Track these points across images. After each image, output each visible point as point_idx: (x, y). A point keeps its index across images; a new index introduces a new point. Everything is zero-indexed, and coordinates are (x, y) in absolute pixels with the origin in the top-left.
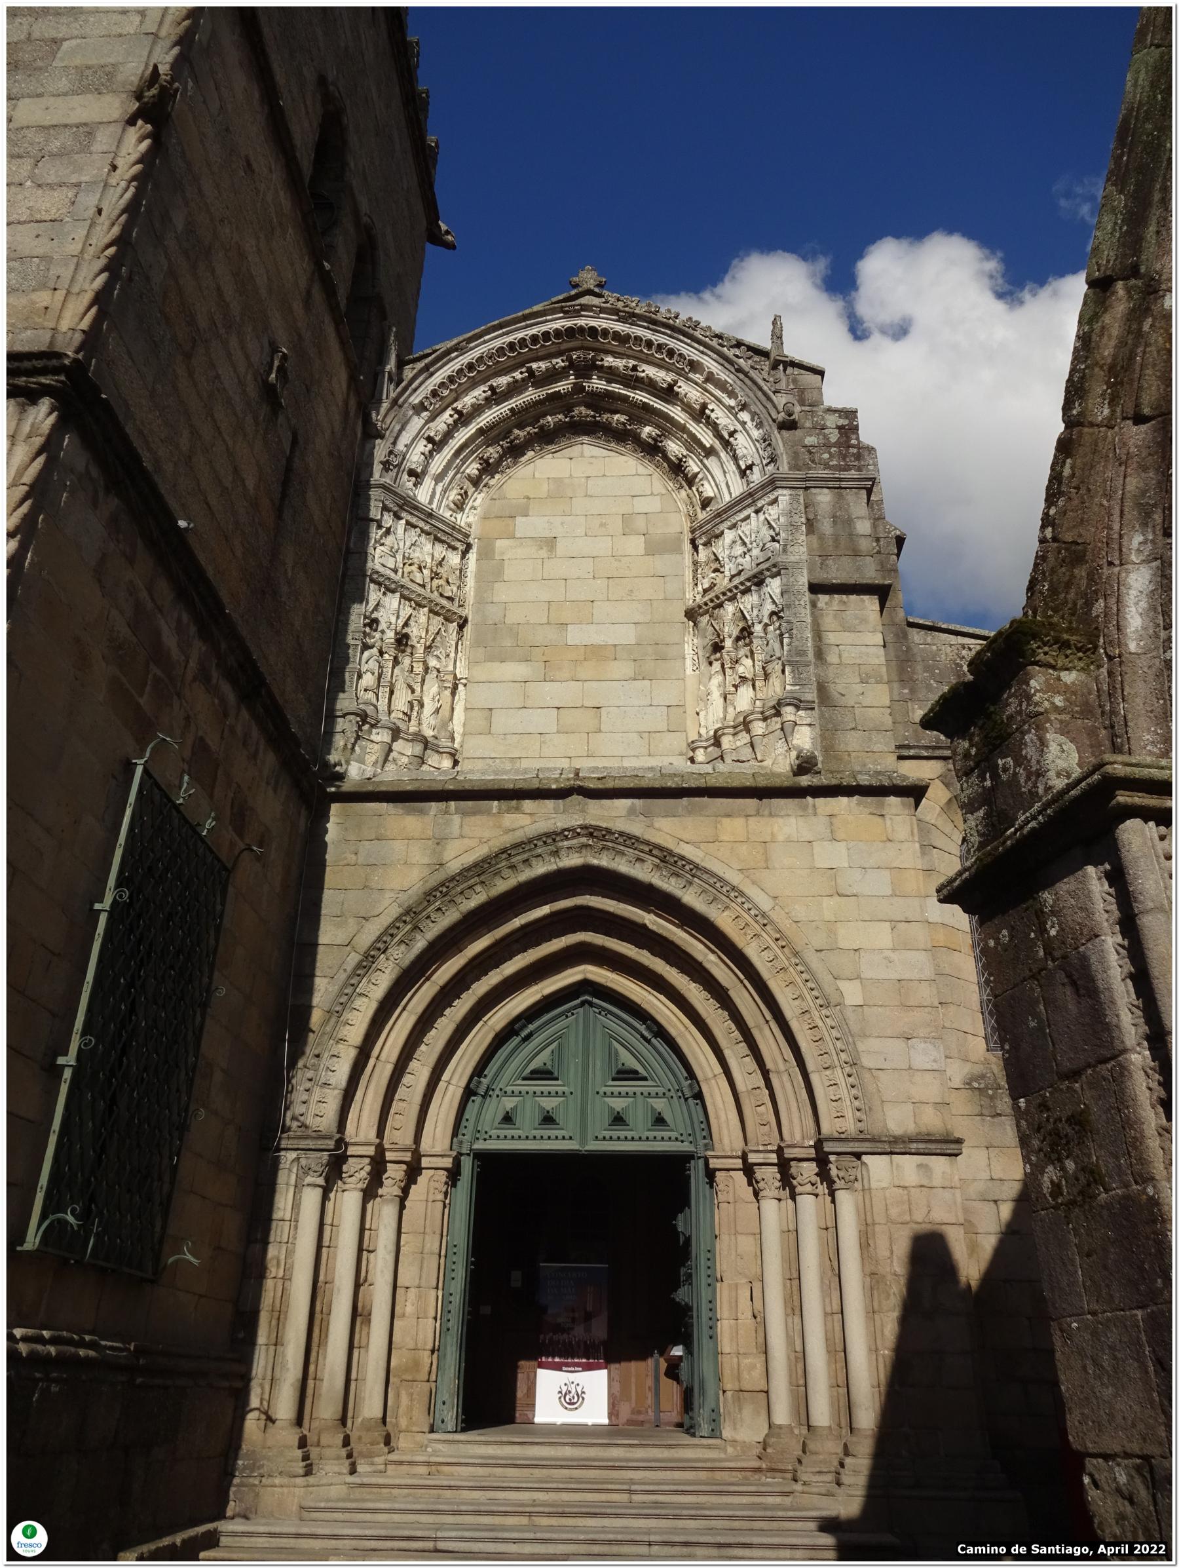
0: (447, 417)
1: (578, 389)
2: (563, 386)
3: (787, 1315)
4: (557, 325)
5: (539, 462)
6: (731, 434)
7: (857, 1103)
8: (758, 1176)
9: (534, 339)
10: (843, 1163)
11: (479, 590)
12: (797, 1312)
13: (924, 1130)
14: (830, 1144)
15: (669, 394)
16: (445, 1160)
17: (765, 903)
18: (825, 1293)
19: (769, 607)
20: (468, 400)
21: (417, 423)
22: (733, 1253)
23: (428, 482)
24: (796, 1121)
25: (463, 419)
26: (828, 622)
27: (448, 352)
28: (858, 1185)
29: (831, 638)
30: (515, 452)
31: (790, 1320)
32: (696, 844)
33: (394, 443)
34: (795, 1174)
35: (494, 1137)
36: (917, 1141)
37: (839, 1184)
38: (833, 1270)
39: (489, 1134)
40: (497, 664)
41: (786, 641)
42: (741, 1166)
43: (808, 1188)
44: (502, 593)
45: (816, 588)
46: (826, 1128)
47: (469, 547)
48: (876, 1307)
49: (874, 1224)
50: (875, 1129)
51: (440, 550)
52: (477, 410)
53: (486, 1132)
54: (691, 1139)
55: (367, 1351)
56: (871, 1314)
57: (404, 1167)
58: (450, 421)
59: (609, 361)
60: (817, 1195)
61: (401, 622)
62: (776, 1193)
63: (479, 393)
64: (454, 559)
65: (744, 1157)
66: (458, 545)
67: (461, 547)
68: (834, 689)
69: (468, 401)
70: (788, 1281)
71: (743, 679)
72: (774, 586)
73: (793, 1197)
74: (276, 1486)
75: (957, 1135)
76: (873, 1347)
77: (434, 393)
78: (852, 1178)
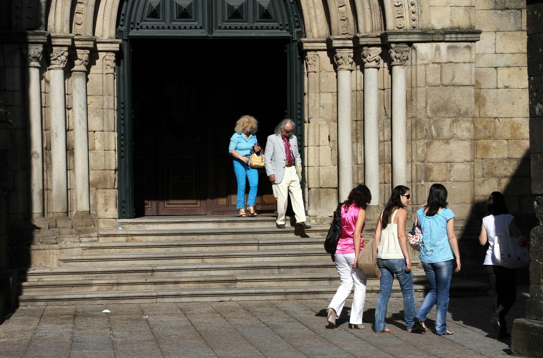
3: (353, 143)
7: (412, 8)
8: (339, 55)
10: (400, 49)
12: (361, 140)
13: (456, 25)
14: (392, 36)
16: (114, 45)
18: (381, 129)
22: (317, 105)
24: (368, 19)
28: (409, 62)
31: (355, 146)
34: (365, 55)
35: (144, 27)
36: (450, 33)
37: (396, 62)
38: (386, 115)
39: (140, 24)
42: (326, 48)
43: (374, 64)
46: (391, 25)
48: (414, 137)
49: (417, 87)
50: (423, 23)
53: (138, 24)
54: (288, 28)
55: (74, 172)
56: (410, 141)
57: (88, 52)
60: (378, 68)
62: (349, 67)
65: (329, 42)
70: (355, 122)
73: (362, 70)
74: (41, 250)
75: (477, 28)
76: (410, 160)
78: (405, 58)
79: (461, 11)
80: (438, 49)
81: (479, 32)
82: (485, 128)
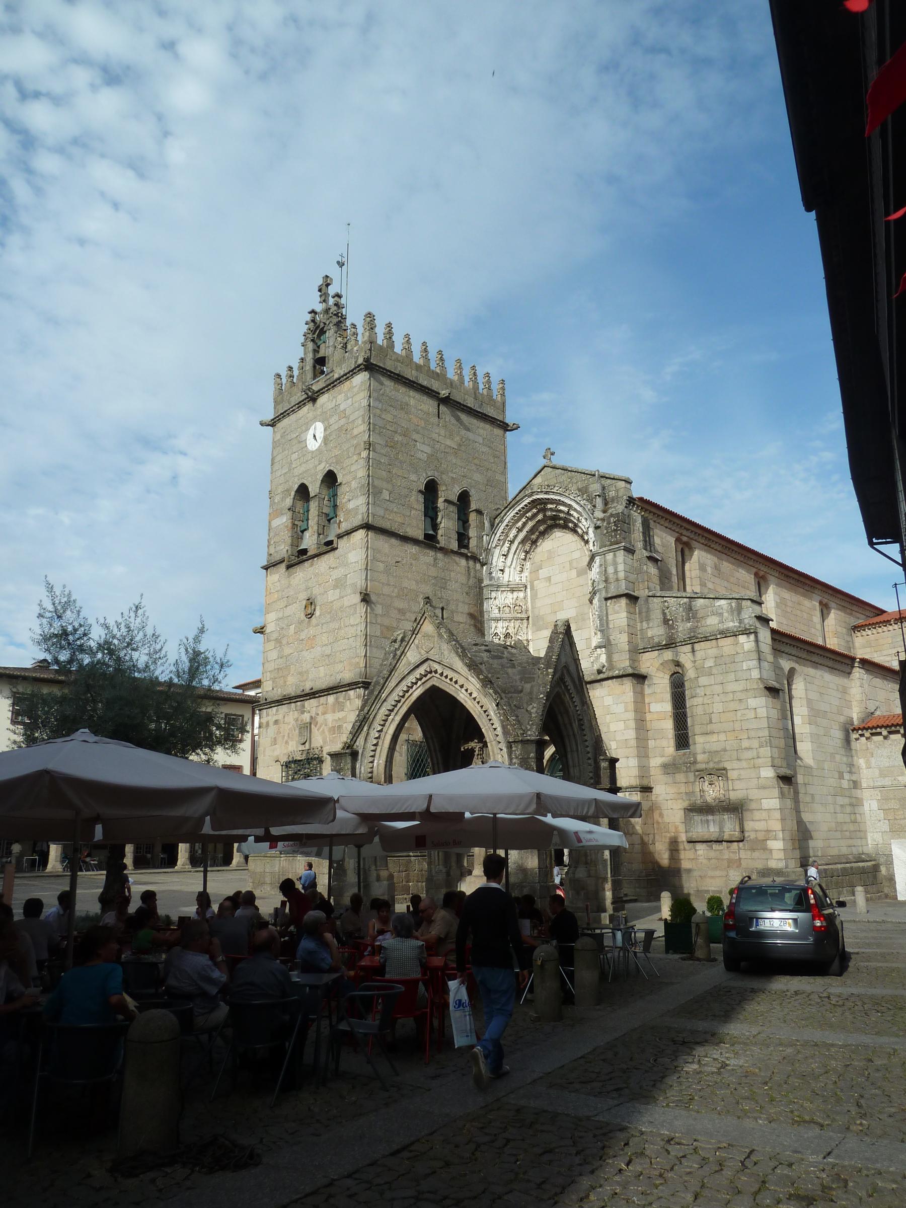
0: (507, 545)
1: (545, 516)
2: (540, 517)
4: (527, 501)
5: (544, 544)
9: (523, 508)
11: (532, 603)
13: (631, 784)
20: (511, 536)
21: (497, 552)
23: (507, 570)
25: (512, 542)
26: (610, 611)
27: (498, 524)
29: (610, 618)
30: (534, 542)
33: (491, 564)
40: (539, 632)
44: (538, 604)
45: (606, 599)
47: (526, 587)
51: (515, 594)
52: (516, 537)
58: (508, 545)
59: (550, 506)
61: (505, 629)
63: (514, 532)
64: (521, 595)
66: (522, 589)
67: (523, 589)
68: (611, 638)
69: (511, 536)
77: (499, 540)
79: (632, 778)
80: (625, 795)
82: (665, 827)
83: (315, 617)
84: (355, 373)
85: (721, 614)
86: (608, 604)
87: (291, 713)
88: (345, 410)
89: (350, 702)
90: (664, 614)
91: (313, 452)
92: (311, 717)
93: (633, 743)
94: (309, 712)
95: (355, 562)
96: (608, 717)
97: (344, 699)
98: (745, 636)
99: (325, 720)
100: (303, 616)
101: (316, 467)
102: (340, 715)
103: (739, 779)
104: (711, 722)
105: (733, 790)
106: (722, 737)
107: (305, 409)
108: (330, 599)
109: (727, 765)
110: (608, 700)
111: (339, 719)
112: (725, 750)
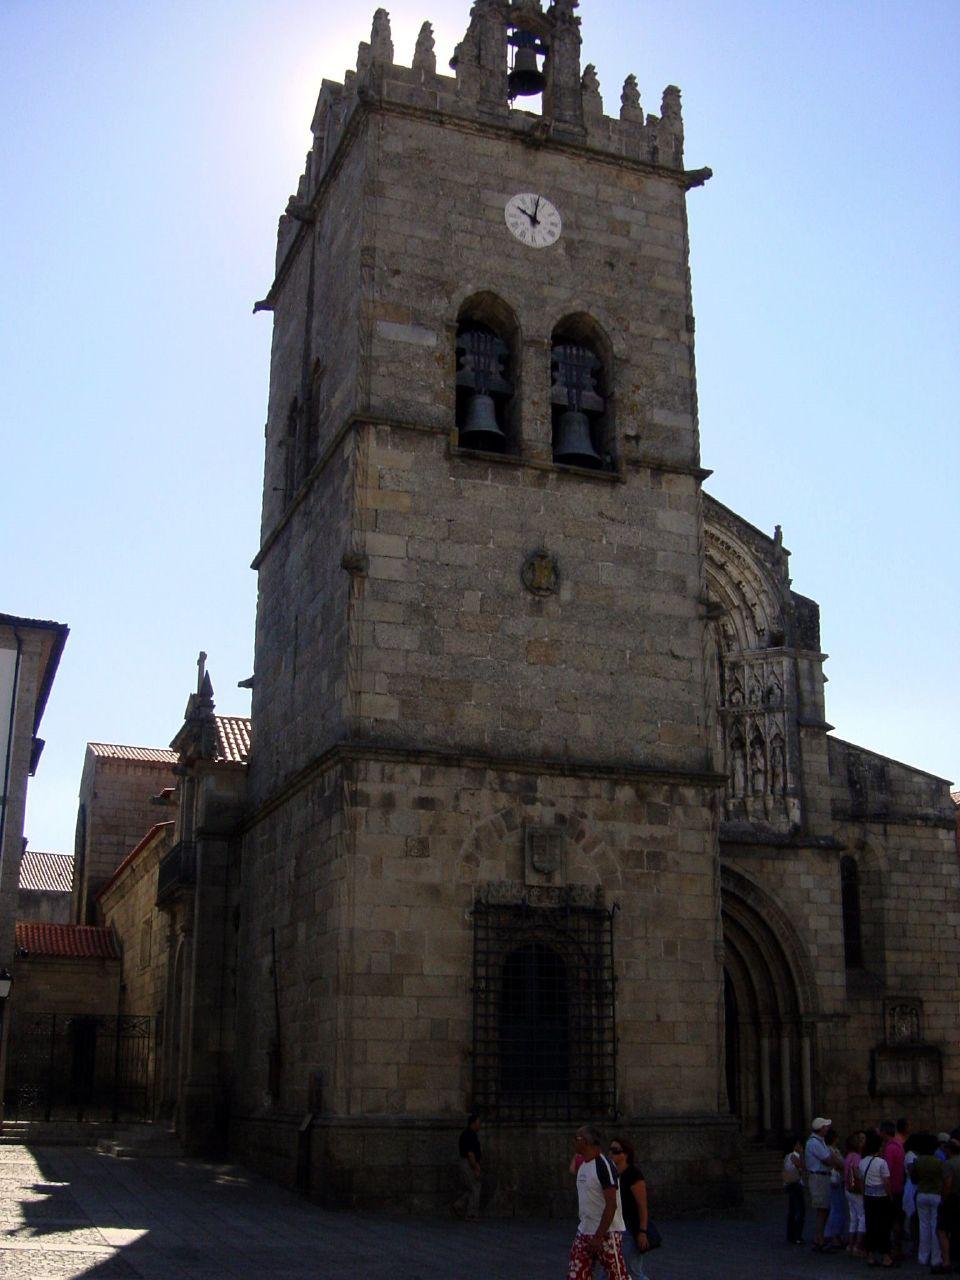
6: (754, 605)
15: (721, 567)
17: (780, 904)
19: (774, 731)
26: (805, 747)
29: (806, 757)
32: (752, 874)
41: (788, 757)
71: (759, 770)
72: (779, 717)
81: (849, 1017)
83: (558, 600)
84: (659, 175)
85: (918, 796)
86: (802, 735)
87: (485, 793)
88: (628, 224)
89: (685, 813)
90: (850, 772)
91: (527, 249)
92: (561, 819)
93: (841, 951)
94: (553, 804)
95: (680, 536)
96: (807, 908)
97: (669, 798)
98: (945, 831)
99: (611, 834)
100: (512, 582)
101: (541, 284)
102: (659, 831)
103: (935, 1015)
104: (905, 936)
105: (929, 1028)
106: (918, 957)
107: (499, 147)
108: (605, 578)
109: (922, 994)
110: (807, 882)
111: (653, 839)
112: (921, 976)
